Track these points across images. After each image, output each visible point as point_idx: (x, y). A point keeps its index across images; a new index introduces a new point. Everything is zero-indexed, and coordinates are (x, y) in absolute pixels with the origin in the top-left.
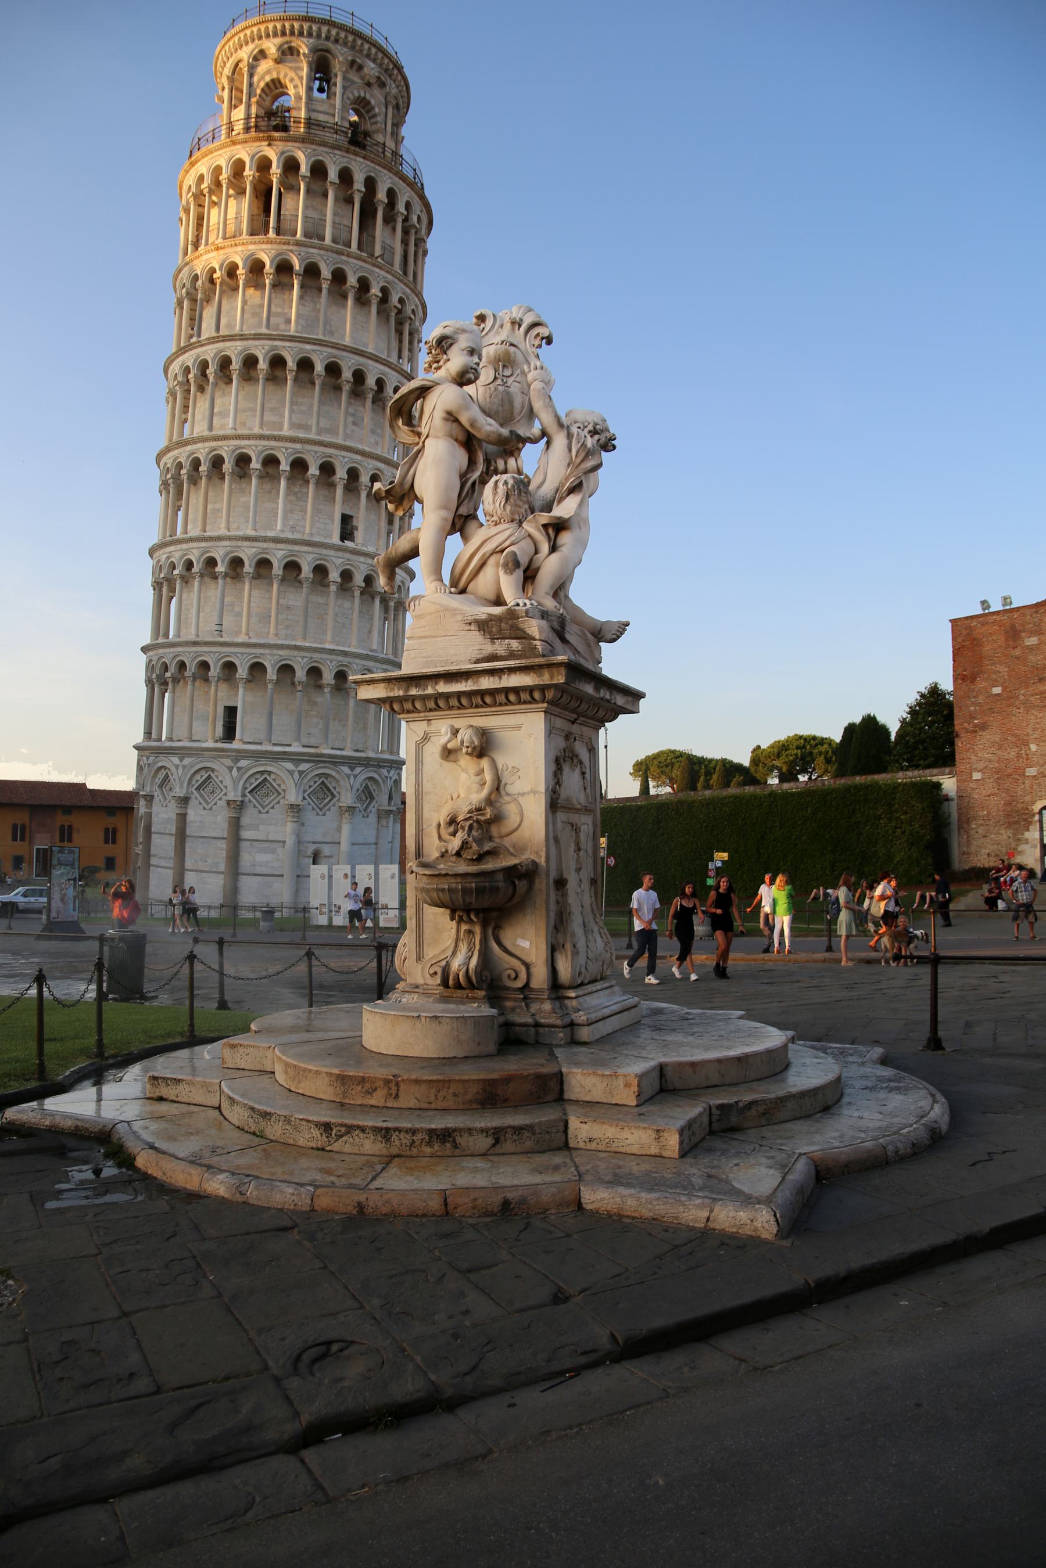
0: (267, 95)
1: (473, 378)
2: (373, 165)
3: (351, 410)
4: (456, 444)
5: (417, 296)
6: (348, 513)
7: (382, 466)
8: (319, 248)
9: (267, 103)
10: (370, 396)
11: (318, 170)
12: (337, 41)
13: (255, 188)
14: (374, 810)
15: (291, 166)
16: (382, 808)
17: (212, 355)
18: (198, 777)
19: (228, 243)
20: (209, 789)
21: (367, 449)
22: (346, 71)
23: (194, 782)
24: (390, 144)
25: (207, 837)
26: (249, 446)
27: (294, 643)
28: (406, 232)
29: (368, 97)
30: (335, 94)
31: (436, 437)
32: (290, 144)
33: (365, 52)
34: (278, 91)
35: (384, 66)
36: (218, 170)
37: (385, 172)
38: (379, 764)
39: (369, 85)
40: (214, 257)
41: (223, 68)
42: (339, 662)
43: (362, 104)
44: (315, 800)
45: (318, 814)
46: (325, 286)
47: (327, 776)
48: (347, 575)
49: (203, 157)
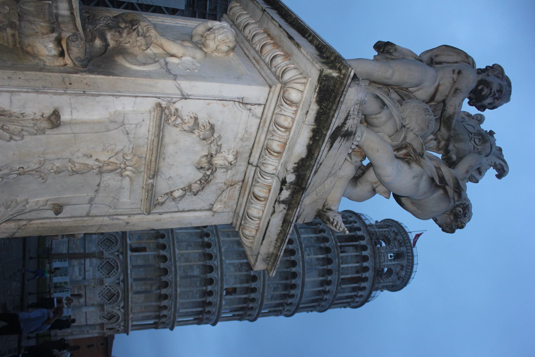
0: (384, 237)
3: (279, 286)
5: (328, 307)
6: (238, 290)
7: (259, 302)
10: (287, 292)
11: (365, 259)
12: (408, 259)
13: (353, 236)
14: (103, 321)
15: (364, 248)
16: (105, 325)
18: (113, 238)
20: (108, 244)
21: (266, 294)
22: (400, 264)
23: (111, 236)
24: (381, 285)
25: (85, 245)
28: (351, 297)
29: (394, 274)
30: (391, 261)
33: (407, 270)
34: (386, 241)
35: (405, 279)
36: (355, 222)
38: (126, 320)
39: (397, 274)
41: (387, 222)
42: (172, 295)
44: (106, 291)
45: (99, 294)
46: (325, 267)
47: (118, 296)
48: (210, 293)
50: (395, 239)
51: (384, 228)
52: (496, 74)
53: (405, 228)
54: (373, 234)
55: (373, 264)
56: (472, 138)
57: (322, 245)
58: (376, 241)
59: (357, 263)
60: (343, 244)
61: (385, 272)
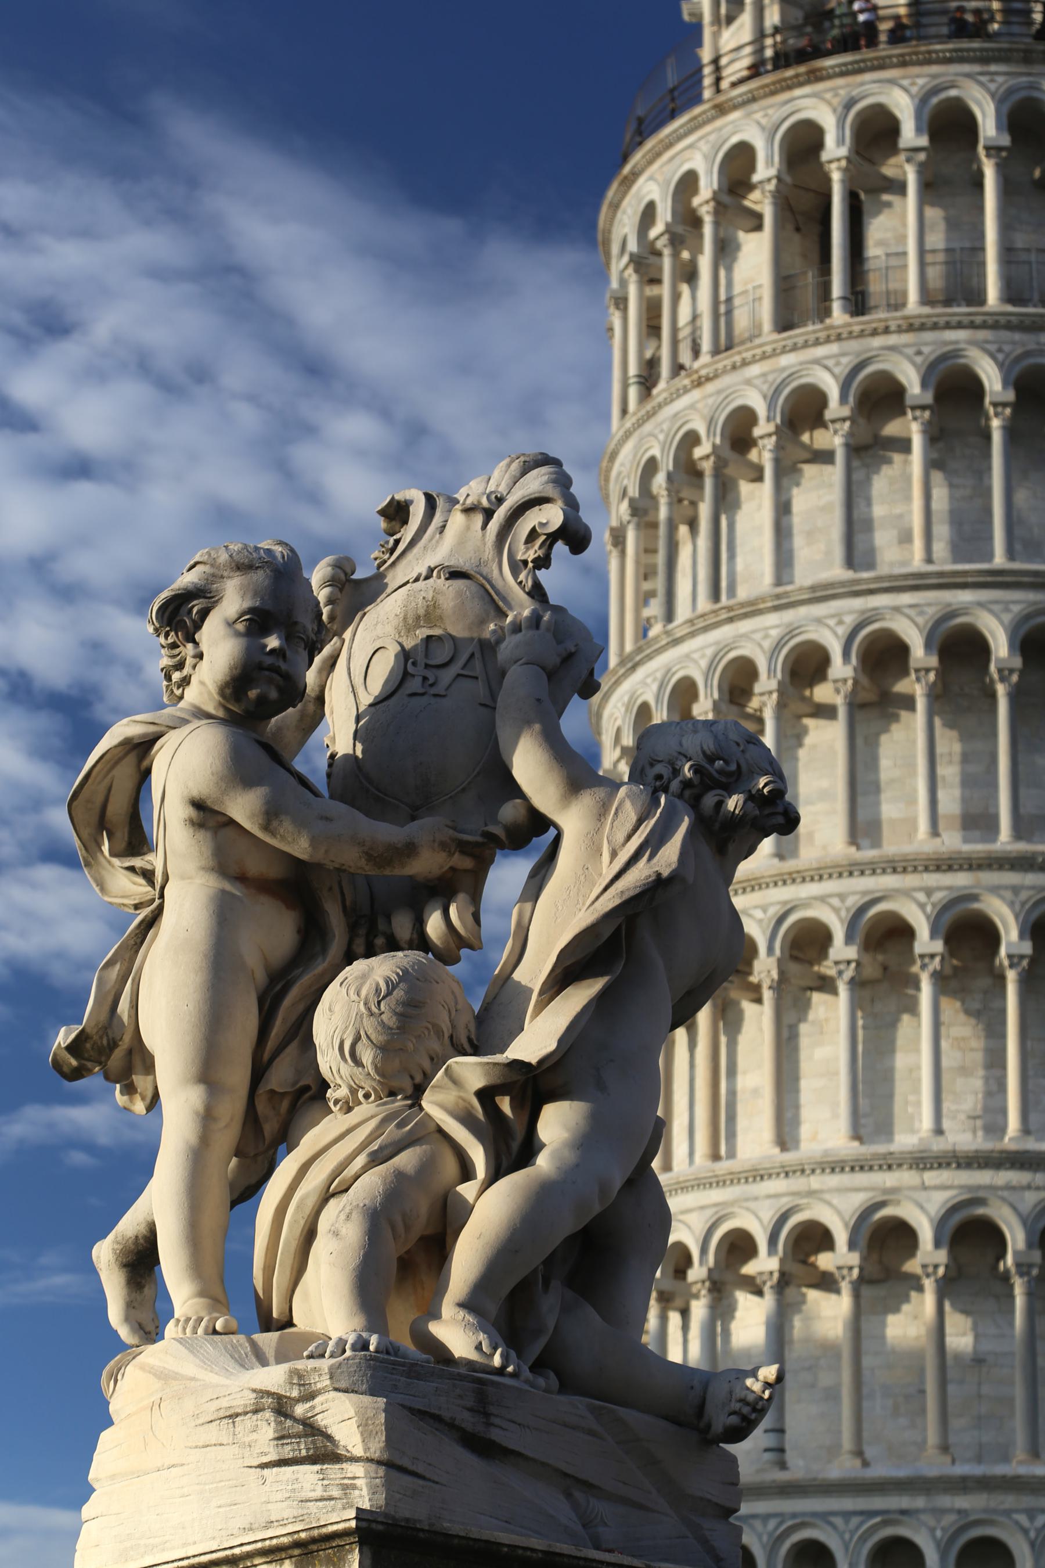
1: (273, 694)
8: (972, 326)
17: (704, 663)
19: (726, 360)
26: (823, 899)
27: (1001, 1470)
31: (183, 877)
32: (868, 77)
36: (688, 182)
40: (692, 407)
49: (650, 162)
52: (193, 621)
55: (993, 68)
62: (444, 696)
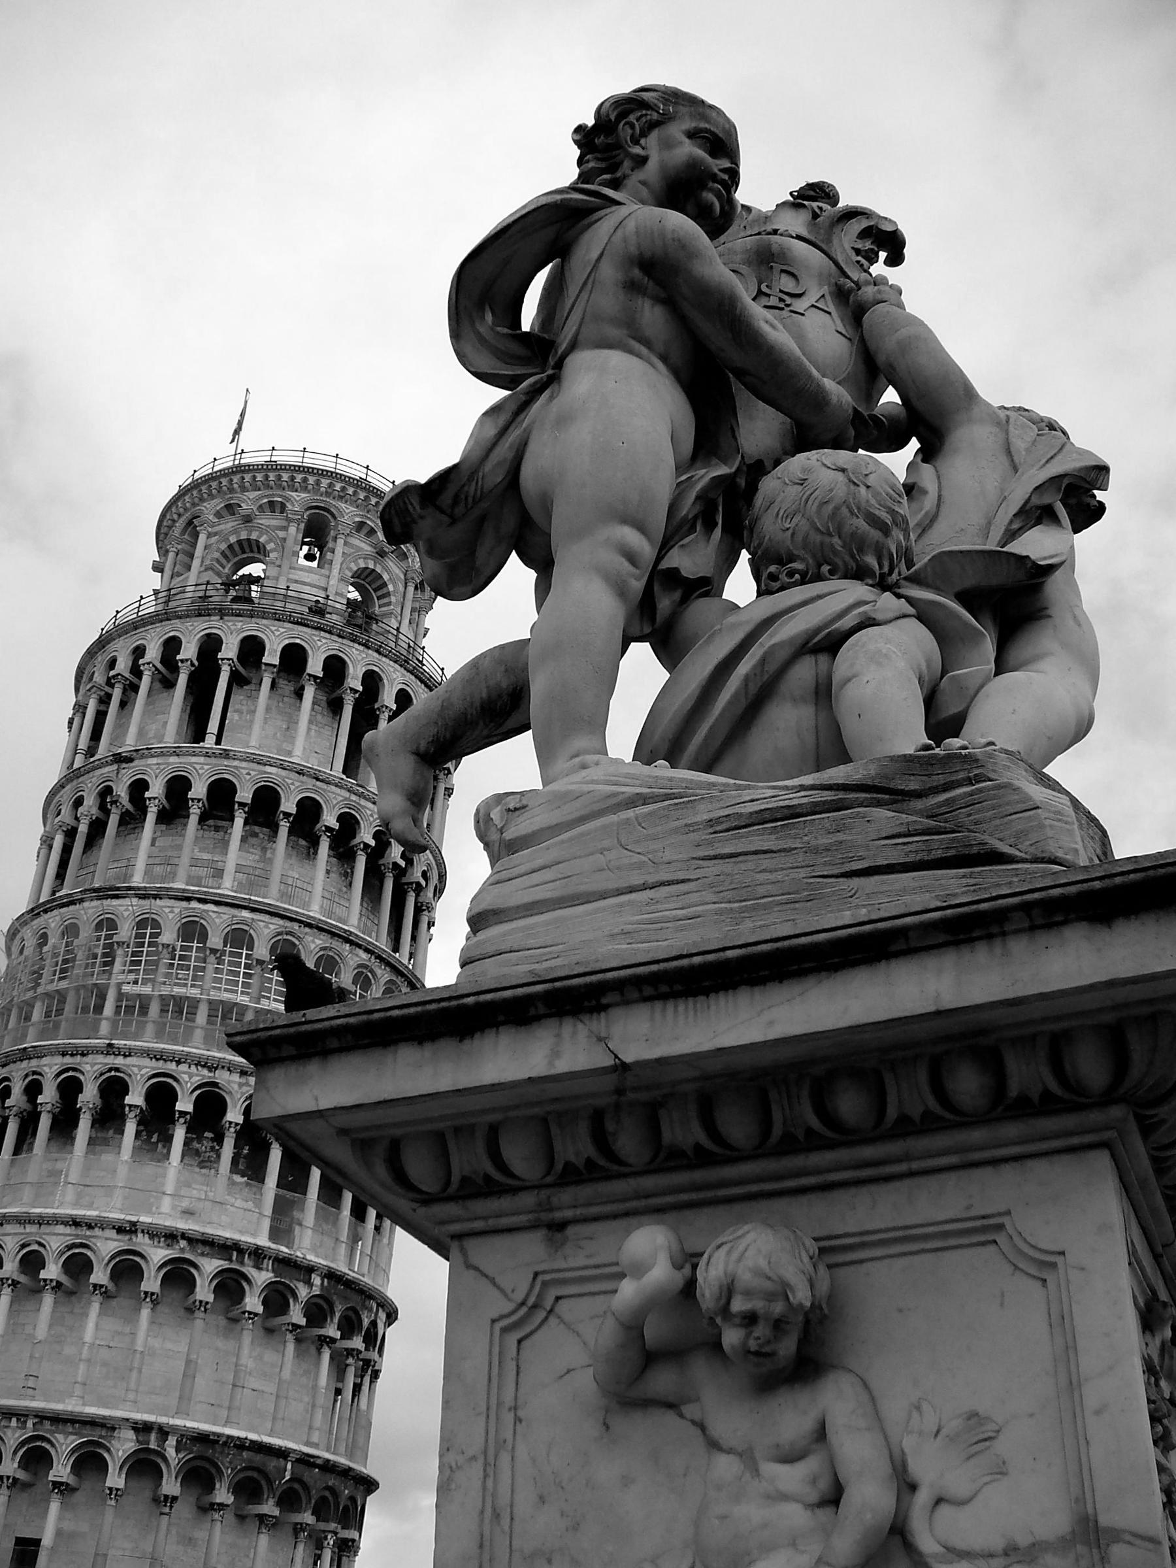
2: (380, 657)
4: (660, 365)
9: (226, 570)
11: (294, 658)
12: (341, 498)
15: (252, 649)
29: (379, 569)
34: (245, 556)
36: (139, 652)
37: (397, 666)
41: (170, 527)
43: (369, 579)
50: (248, 519)
51: (194, 545)
53: (216, 469)
54: (205, 598)
55: (322, 634)
56: (781, 300)
57: (195, 811)
58: (233, 593)
59: (299, 693)
60: (213, 726)
61: (360, 599)
62: (803, 315)
